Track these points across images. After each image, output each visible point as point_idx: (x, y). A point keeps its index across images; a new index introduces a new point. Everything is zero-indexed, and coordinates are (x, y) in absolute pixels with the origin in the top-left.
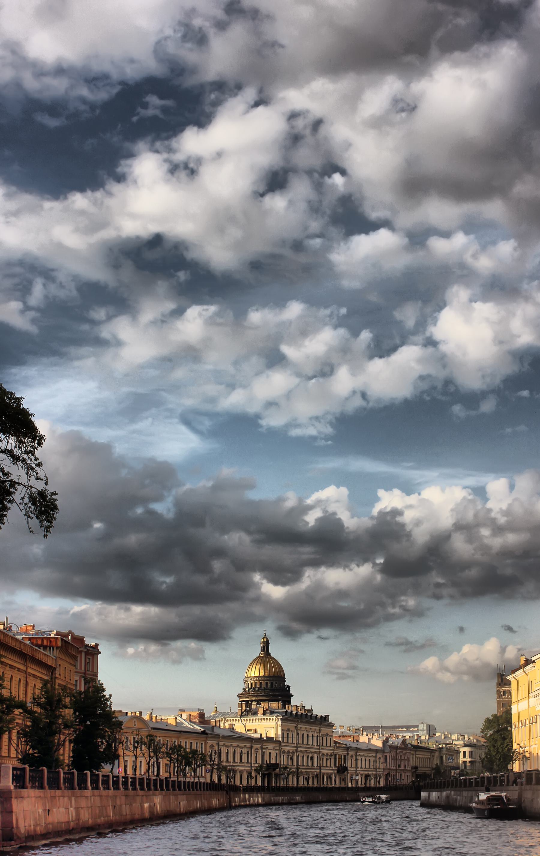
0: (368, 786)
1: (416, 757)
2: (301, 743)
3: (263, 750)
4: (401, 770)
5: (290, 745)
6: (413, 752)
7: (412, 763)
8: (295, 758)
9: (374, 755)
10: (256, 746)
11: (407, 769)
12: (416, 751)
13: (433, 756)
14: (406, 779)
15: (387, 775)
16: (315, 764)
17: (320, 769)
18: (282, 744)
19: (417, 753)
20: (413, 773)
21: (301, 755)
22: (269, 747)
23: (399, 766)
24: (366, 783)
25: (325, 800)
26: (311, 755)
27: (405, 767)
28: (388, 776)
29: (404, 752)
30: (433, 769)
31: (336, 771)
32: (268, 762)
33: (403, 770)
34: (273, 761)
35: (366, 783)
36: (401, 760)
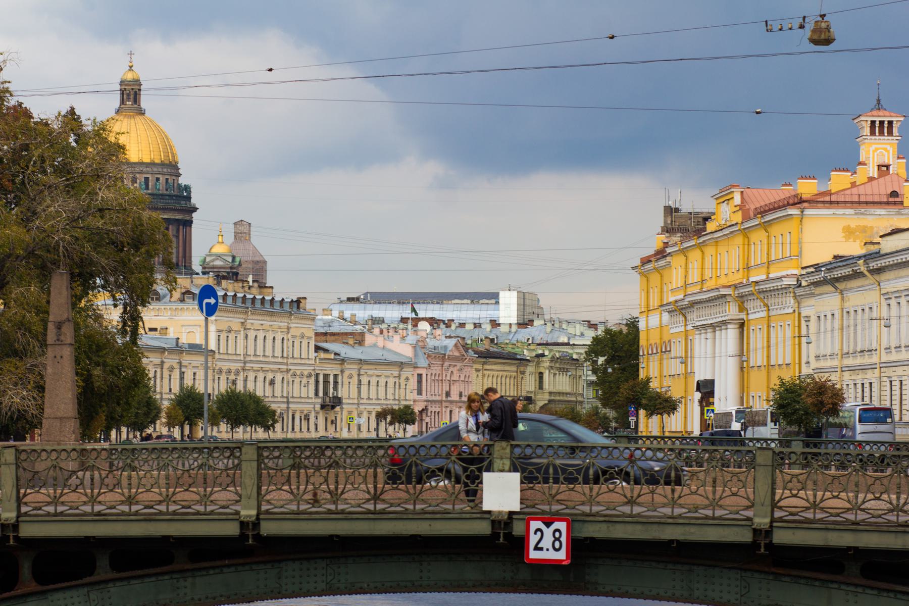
1: (484, 375)
4: (451, 402)
6: (480, 367)
12: (484, 363)
13: (523, 373)
17: (288, 402)
18: (217, 356)
19: (486, 367)
23: (448, 394)
24: (377, 429)
26: (270, 376)
28: (424, 415)
29: (459, 365)
31: (318, 407)
33: (456, 402)
35: (377, 429)
36: (451, 382)
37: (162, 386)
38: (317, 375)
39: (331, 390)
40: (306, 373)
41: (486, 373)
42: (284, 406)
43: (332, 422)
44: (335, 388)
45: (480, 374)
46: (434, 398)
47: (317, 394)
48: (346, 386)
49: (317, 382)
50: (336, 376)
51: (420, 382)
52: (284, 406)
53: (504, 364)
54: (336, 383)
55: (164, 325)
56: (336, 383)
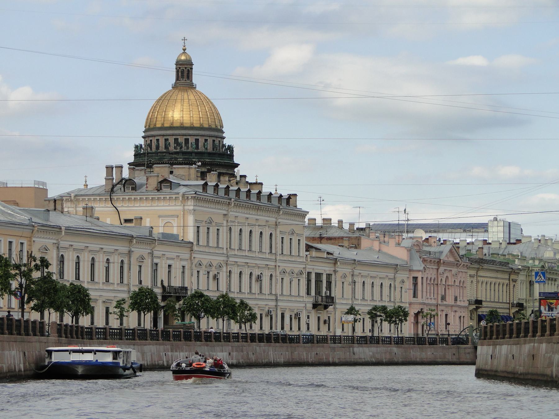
0: (376, 334)
1: (478, 282)
2: (237, 247)
3: (156, 261)
4: (447, 306)
5: (212, 250)
6: (473, 272)
7: (470, 294)
8: (223, 277)
9: (391, 275)
10: (139, 251)
11: (458, 303)
12: (478, 269)
13: (515, 281)
14: (458, 323)
15: (417, 315)
16: (266, 290)
17: (277, 300)
18: (195, 248)
19: (481, 273)
20: (471, 312)
21: (235, 271)
22: (168, 255)
23: (443, 298)
24: (372, 331)
25: (282, 360)
26: (256, 272)
27: (456, 299)
28: (420, 318)
29: (454, 270)
30: (513, 305)
31: (310, 306)
32: (166, 284)
33: (452, 306)
34: (176, 283)
35: (372, 331)
36: (447, 287)
37: (129, 277)
38: (309, 274)
39: (324, 289)
40: (296, 271)
41: (481, 279)
42: (273, 304)
43: (325, 322)
44: (329, 287)
45: (475, 280)
46: (429, 301)
47: (308, 293)
48: (339, 285)
49: (309, 281)
50: (329, 276)
51: (415, 285)
52: (273, 304)
53: (497, 271)
54: (329, 283)
55: (138, 216)
56: (329, 283)
